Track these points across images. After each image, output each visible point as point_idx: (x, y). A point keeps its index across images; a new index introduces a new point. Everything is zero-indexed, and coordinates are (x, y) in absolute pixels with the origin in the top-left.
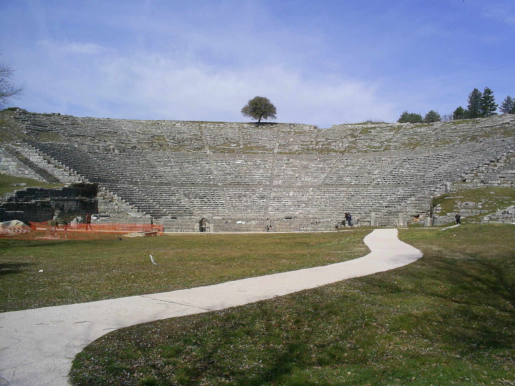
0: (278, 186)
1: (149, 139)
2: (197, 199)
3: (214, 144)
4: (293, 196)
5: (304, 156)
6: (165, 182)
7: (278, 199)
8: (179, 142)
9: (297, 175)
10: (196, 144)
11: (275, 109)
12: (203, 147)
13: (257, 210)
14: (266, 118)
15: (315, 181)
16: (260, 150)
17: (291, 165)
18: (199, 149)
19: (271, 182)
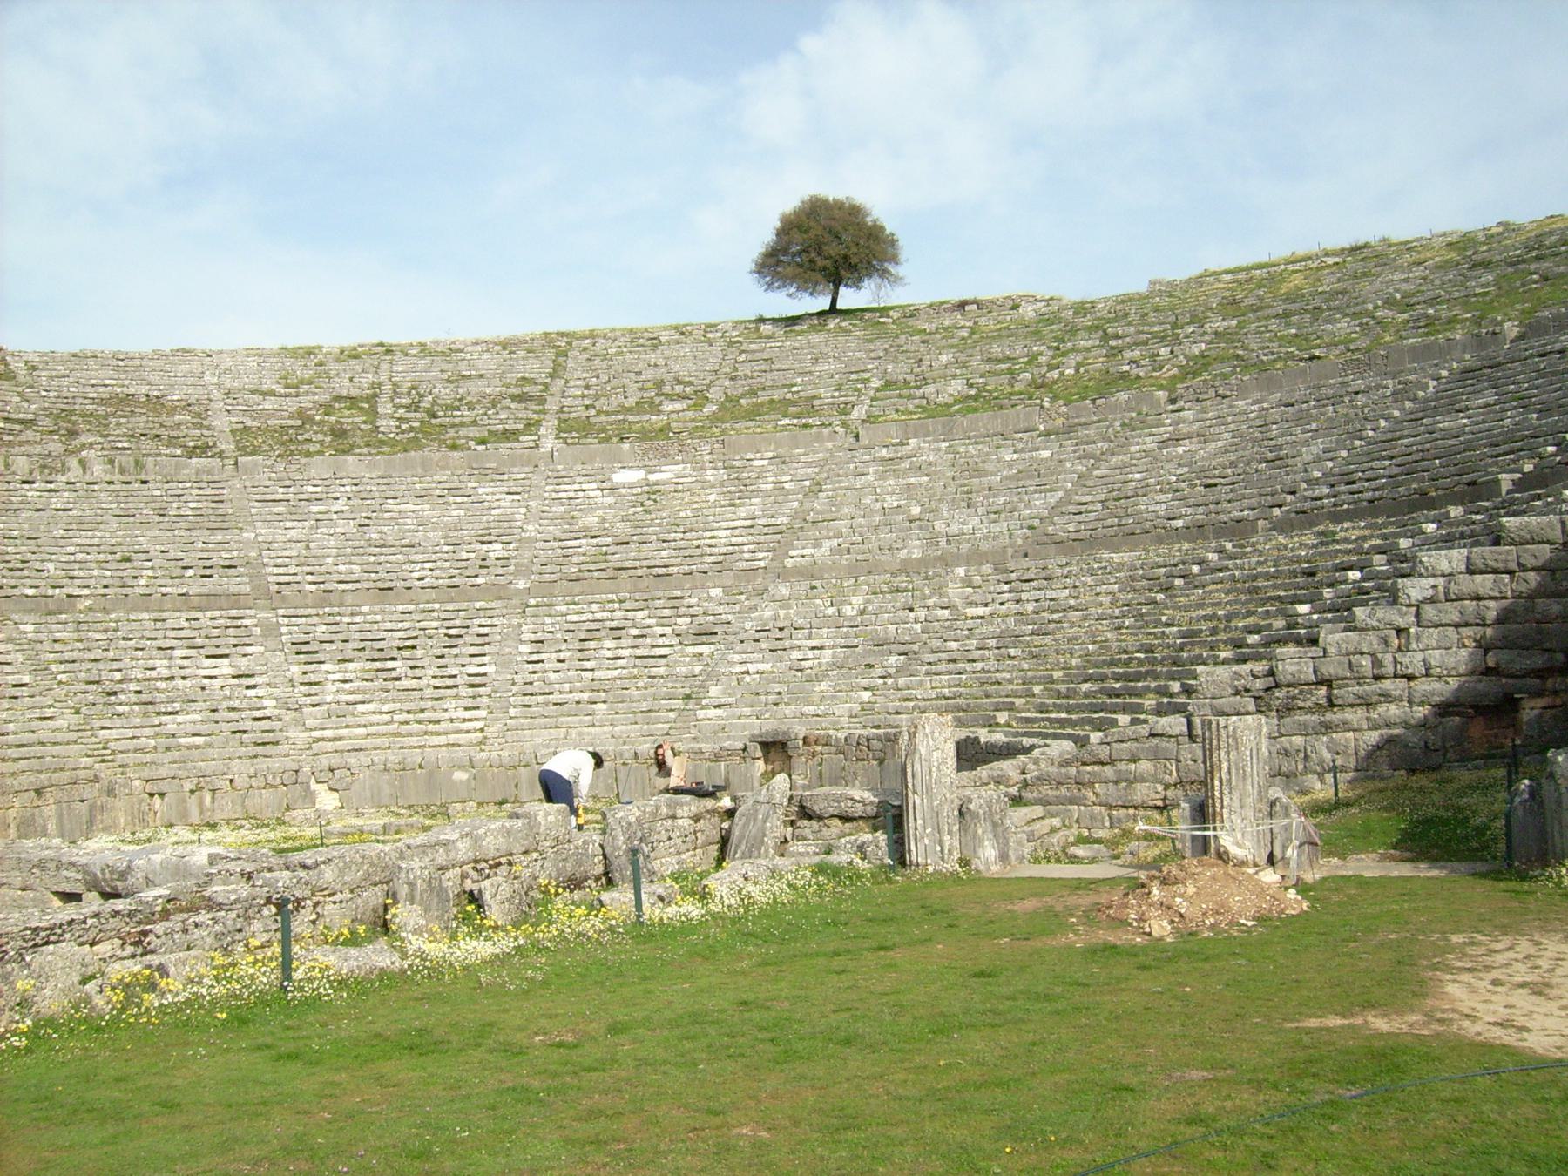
0: (809, 573)
1: (301, 414)
2: (351, 666)
3: (587, 407)
4: (862, 613)
5: (985, 420)
6: (235, 589)
7: (776, 637)
8: (434, 416)
9: (916, 511)
10: (502, 419)
11: (892, 242)
12: (531, 426)
13: (644, 706)
14: (857, 284)
15: (996, 528)
16: (784, 416)
17: (906, 464)
18: (509, 435)
19: (780, 552)
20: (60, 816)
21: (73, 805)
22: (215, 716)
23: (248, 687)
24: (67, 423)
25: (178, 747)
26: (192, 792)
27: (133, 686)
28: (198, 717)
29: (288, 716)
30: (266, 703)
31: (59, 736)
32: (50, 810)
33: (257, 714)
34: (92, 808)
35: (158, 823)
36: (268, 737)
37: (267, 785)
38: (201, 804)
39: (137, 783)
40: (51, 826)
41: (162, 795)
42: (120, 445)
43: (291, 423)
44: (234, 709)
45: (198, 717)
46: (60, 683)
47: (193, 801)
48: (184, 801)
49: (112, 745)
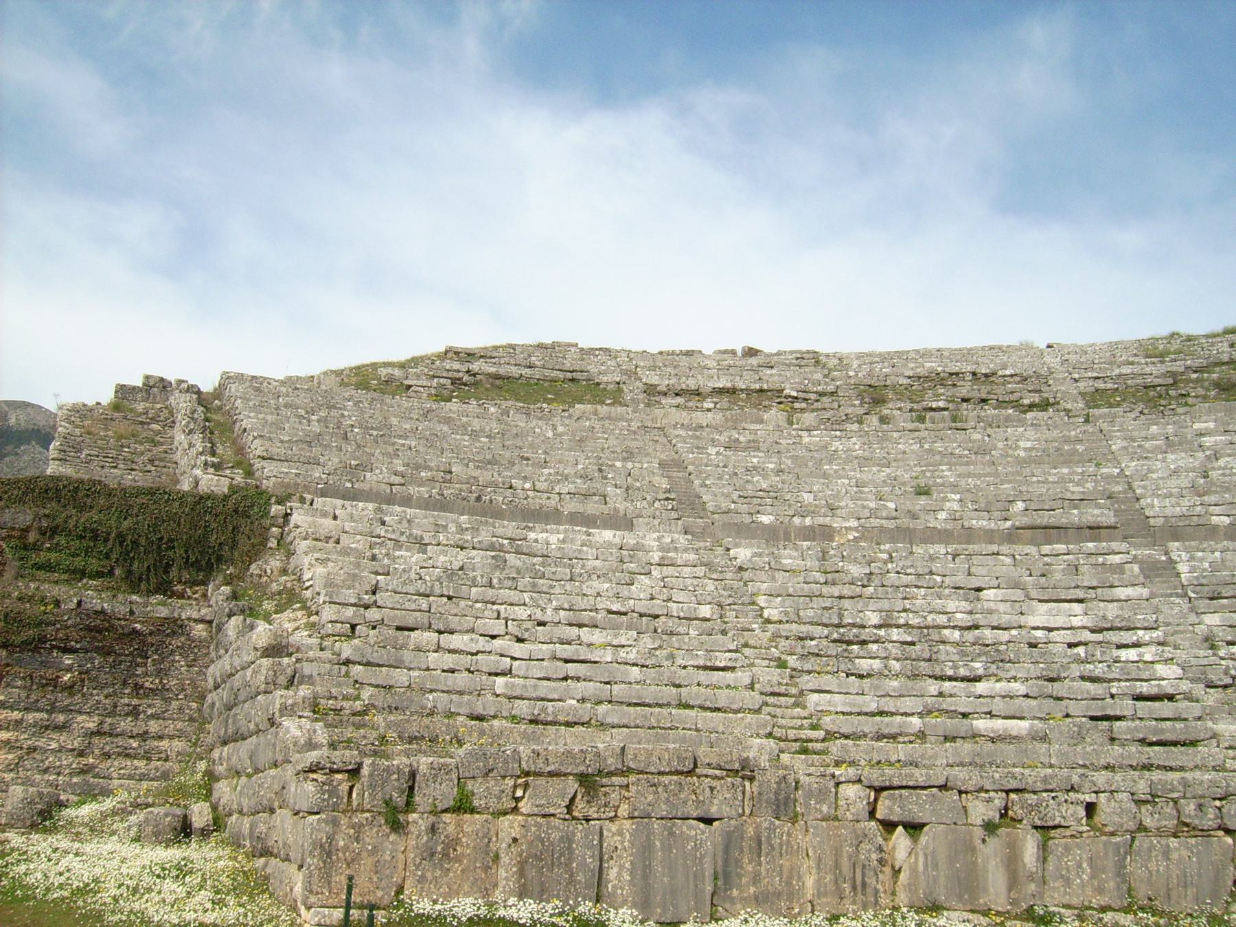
20: (645, 851)
21: (682, 827)
22: (1057, 688)
23: (1119, 647)
24: (875, 395)
25: (975, 736)
26: (990, 827)
27: (895, 634)
28: (1019, 688)
29: (1212, 698)
30: (1161, 669)
31: (723, 698)
32: (620, 834)
33: (1144, 688)
34: (730, 842)
35: (902, 898)
36: (1171, 730)
37: (1183, 828)
38: (1012, 861)
39: (850, 791)
40: (617, 875)
41: (914, 828)
42: (934, 405)
43: (1160, 381)
44: (1093, 680)
45: (1019, 688)
46: (768, 621)
47: (990, 853)
48: (973, 850)
49: (827, 720)
